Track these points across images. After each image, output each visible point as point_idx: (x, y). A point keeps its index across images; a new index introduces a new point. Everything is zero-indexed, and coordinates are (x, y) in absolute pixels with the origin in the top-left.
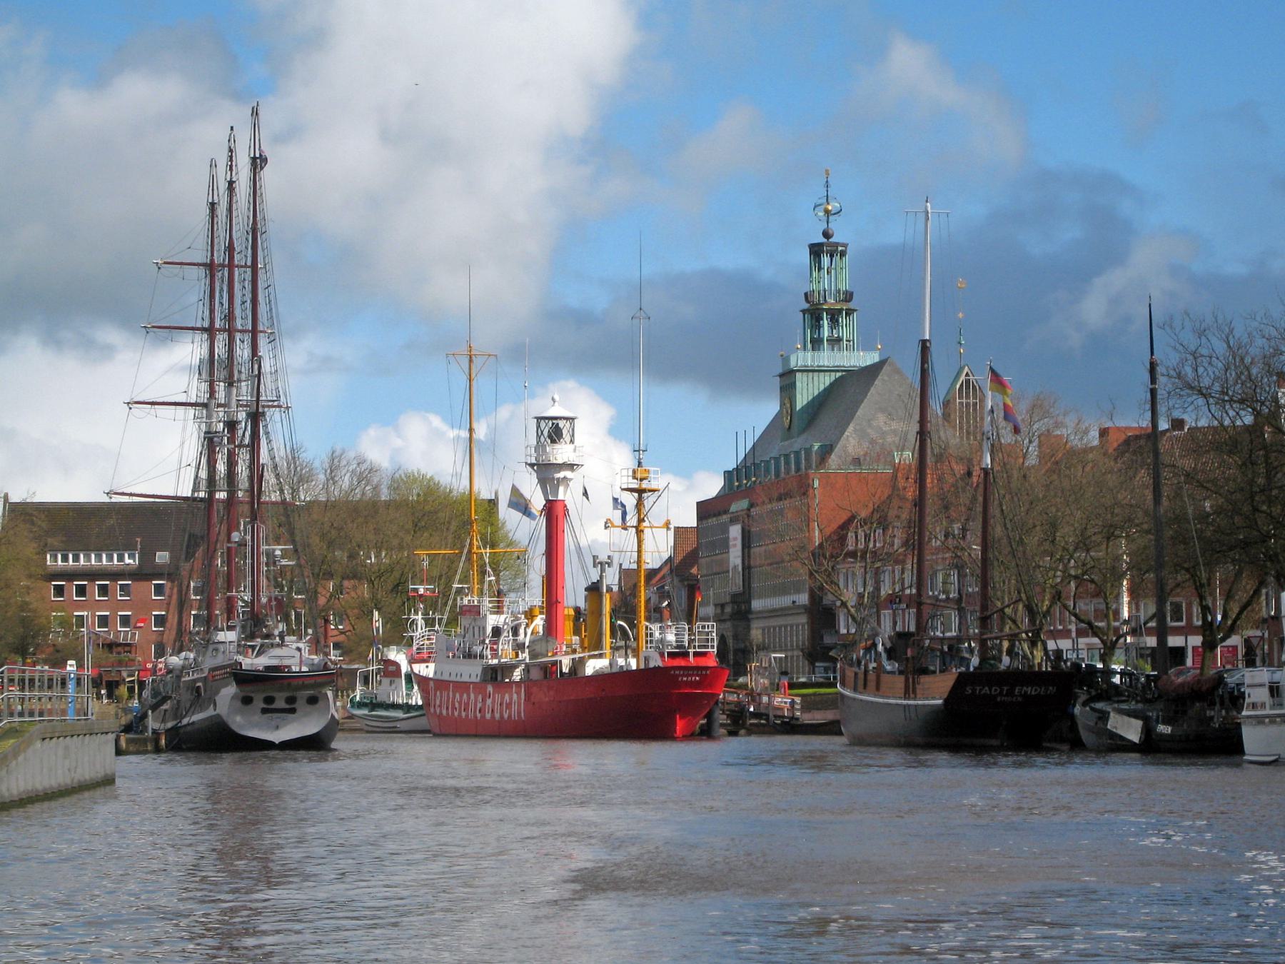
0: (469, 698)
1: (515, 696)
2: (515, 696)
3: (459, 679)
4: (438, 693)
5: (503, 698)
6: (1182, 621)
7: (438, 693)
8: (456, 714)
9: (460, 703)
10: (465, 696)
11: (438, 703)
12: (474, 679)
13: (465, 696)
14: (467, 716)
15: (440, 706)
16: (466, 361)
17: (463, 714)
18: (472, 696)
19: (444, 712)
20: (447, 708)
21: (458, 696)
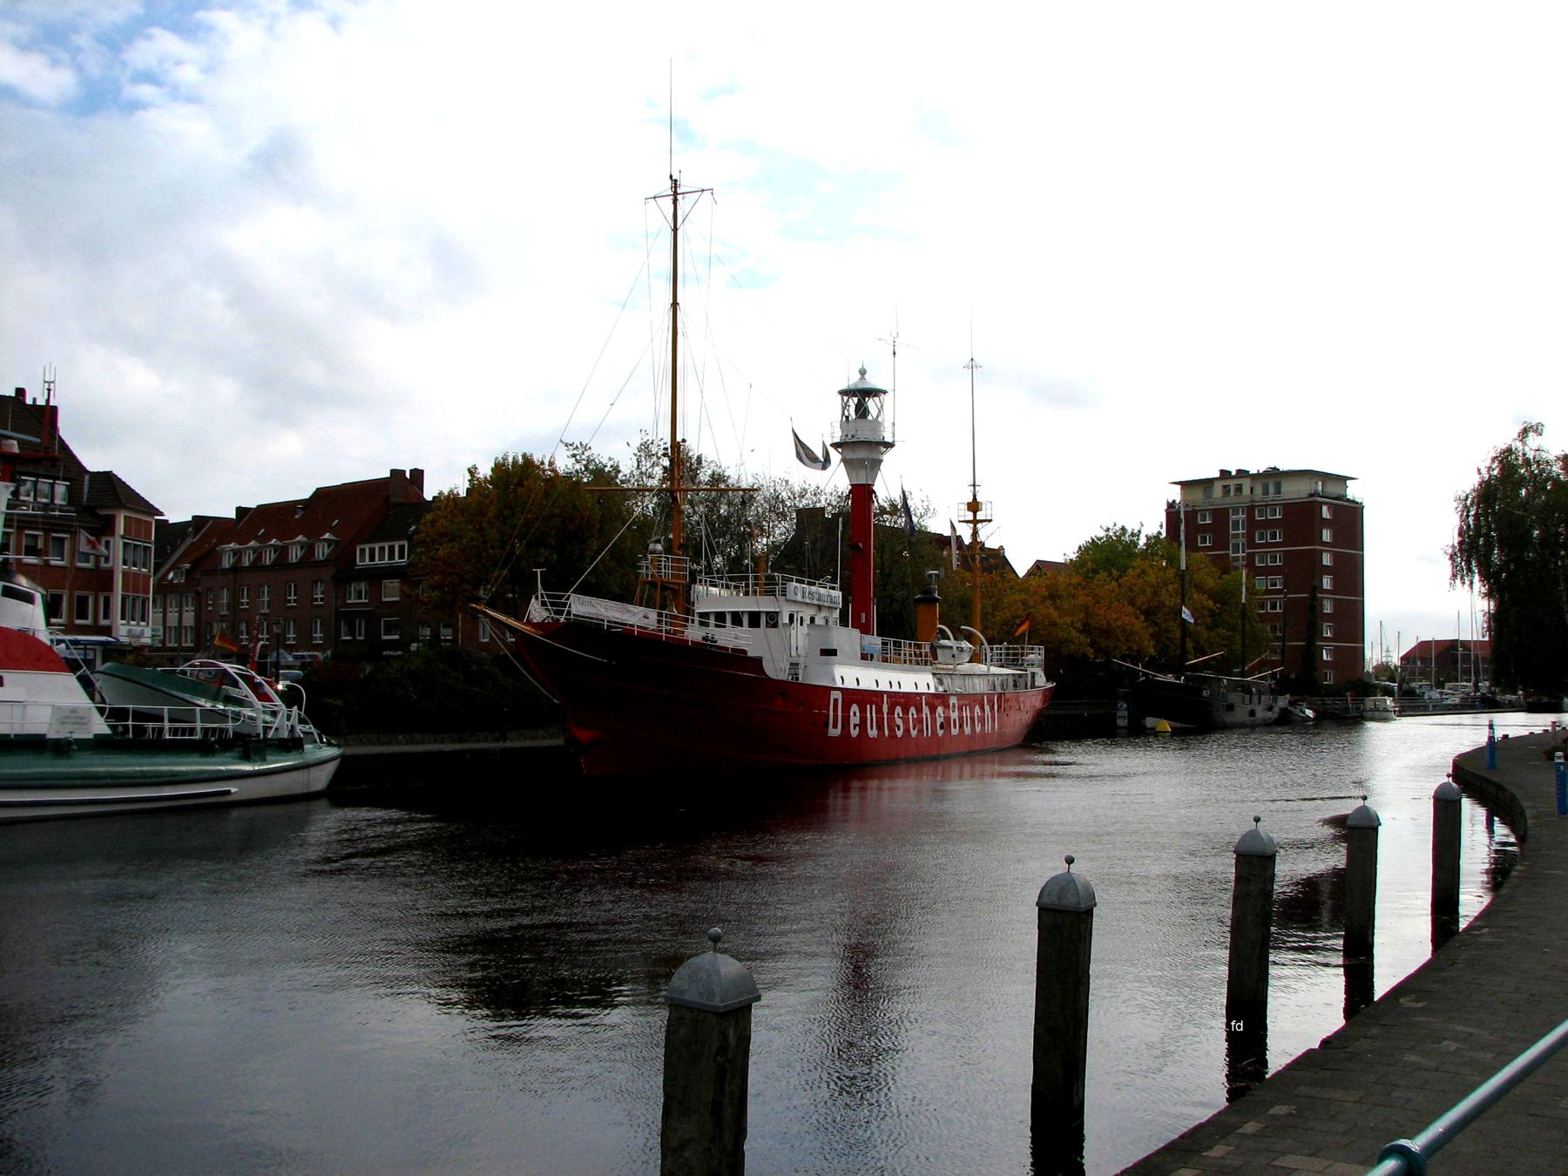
0: (919, 710)
1: (987, 708)
2: (987, 708)
3: (895, 689)
4: (855, 708)
5: (972, 711)
6: (78, 597)
7: (855, 708)
8: (900, 733)
9: (906, 721)
10: (912, 710)
11: (854, 720)
12: (922, 689)
13: (912, 710)
14: (920, 731)
15: (862, 725)
16: (667, 203)
17: (914, 733)
18: (926, 710)
19: (873, 733)
20: (880, 728)
21: (898, 710)
